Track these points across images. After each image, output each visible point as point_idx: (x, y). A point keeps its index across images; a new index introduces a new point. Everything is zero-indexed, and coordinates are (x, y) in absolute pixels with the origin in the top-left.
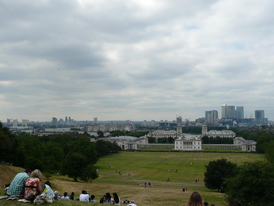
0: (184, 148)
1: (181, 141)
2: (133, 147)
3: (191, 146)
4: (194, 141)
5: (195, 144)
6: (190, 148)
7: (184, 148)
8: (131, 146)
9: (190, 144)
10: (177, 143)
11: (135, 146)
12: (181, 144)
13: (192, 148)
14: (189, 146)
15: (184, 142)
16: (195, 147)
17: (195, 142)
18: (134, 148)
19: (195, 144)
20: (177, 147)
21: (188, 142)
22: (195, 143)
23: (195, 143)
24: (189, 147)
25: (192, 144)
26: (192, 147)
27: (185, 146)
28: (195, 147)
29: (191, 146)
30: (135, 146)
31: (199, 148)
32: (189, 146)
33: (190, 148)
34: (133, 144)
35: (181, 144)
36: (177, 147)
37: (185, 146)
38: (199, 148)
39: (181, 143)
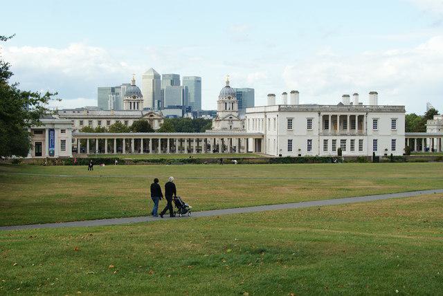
0: (325, 148)
1: (312, 110)
2: (52, 145)
3: (357, 139)
4: (372, 111)
5: (375, 126)
6: (352, 148)
7: (325, 148)
8: (38, 138)
9: (353, 127)
10: (290, 121)
11: (63, 142)
12: (309, 126)
13: (361, 149)
14: (348, 139)
15: (325, 119)
16: (375, 141)
17: (376, 115)
18: (59, 153)
19: (375, 126)
20: (290, 142)
21: (343, 118)
22: (375, 121)
23: (375, 121)
24: (348, 144)
25: (360, 127)
26: (361, 141)
27: (330, 139)
28: (375, 141)
29: (357, 139)
30: (63, 142)
31: (394, 149)
32: (348, 139)
33: (352, 148)
34: (52, 130)
35: (309, 126)
36: (290, 142)
37: (330, 139)
38: (394, 149)
39: (310, 121)
